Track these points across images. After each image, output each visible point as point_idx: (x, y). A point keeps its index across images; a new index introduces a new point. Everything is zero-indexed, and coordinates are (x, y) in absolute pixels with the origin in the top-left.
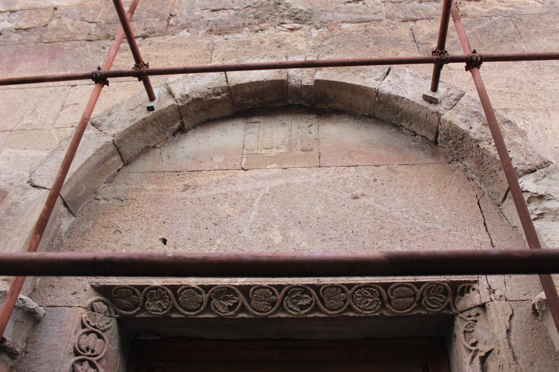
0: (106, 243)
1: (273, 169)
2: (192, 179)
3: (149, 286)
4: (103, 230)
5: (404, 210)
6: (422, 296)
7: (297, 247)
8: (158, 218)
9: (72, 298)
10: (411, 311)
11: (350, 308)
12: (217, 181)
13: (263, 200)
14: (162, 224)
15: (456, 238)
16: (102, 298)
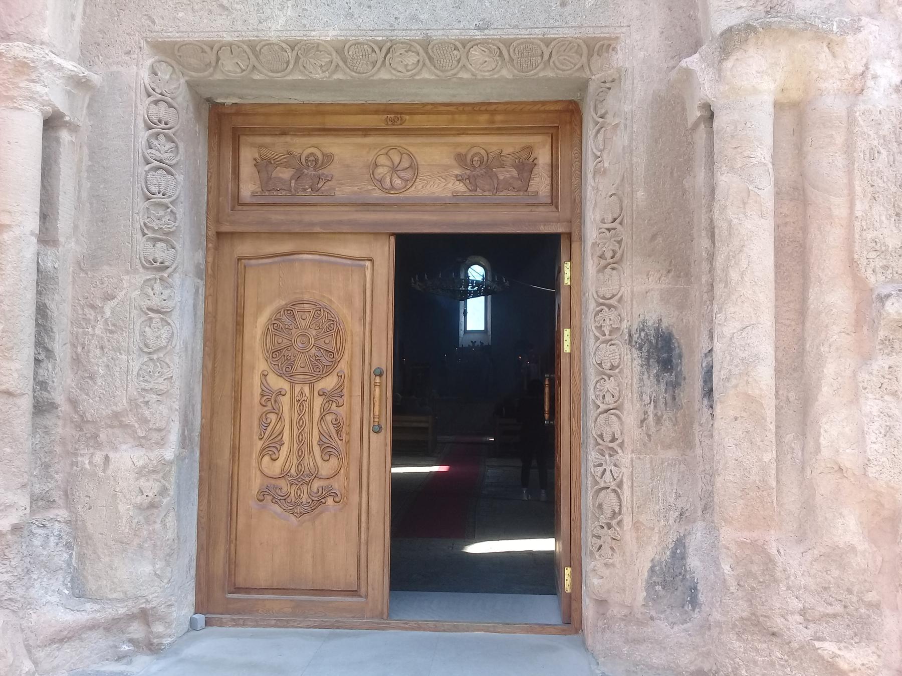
3: (219, 41)
6: (550, 57)
10: (536, 74)
16: (163, 58)
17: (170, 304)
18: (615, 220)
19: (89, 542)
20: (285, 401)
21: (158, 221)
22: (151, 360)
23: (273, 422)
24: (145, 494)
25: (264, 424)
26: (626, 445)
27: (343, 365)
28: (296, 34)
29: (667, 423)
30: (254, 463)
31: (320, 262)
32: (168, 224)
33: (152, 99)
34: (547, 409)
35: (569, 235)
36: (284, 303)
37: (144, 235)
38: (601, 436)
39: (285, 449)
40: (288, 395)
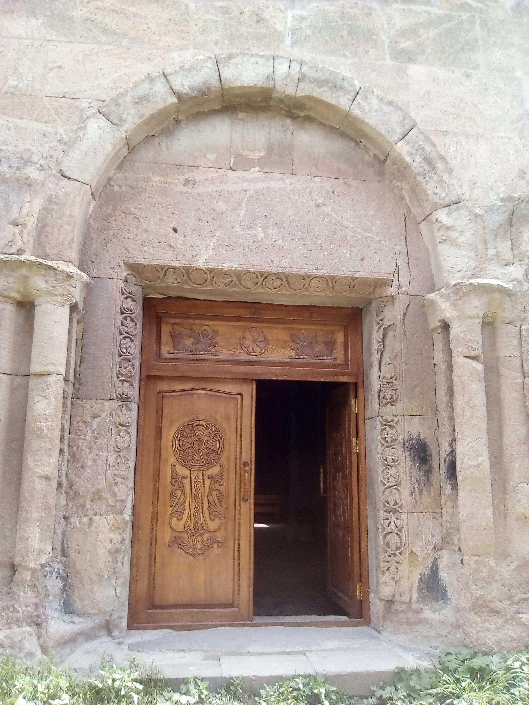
0: (128, 228)
1: (256, 172)
2: (190, 175)
4: (123, 216)
5: (352, 220)
6: (354, 286)
7: (274, 243)
8: (167, 208)
9: (111, 271)
10: (345, 295)
11: (307, 290)
12: (211, 179)
13: (249, 201)
14: (171, 214)
15: (384, 247)
16: (131, 272)
17: (130, 420)
18: (392, 378)
19: (78, 575)
20: (187, 482)
21: (125, 370)
22: (119, 456)
23: (179, 495)
24: (113, 543)
25: (172, 495)
26: (403, 507)
27: (223, 460)
28: (213, 265)
29: (426, 494)
30: (167, 523)
31: (209, 395)
32: (130, 371)
33: (124, 296)
34: (322, 486)
35: (356, 385)
36: (187, 420)
37: (118, 378)
38: (388, 502)
39: (186, 513)
40: (189, 479)
